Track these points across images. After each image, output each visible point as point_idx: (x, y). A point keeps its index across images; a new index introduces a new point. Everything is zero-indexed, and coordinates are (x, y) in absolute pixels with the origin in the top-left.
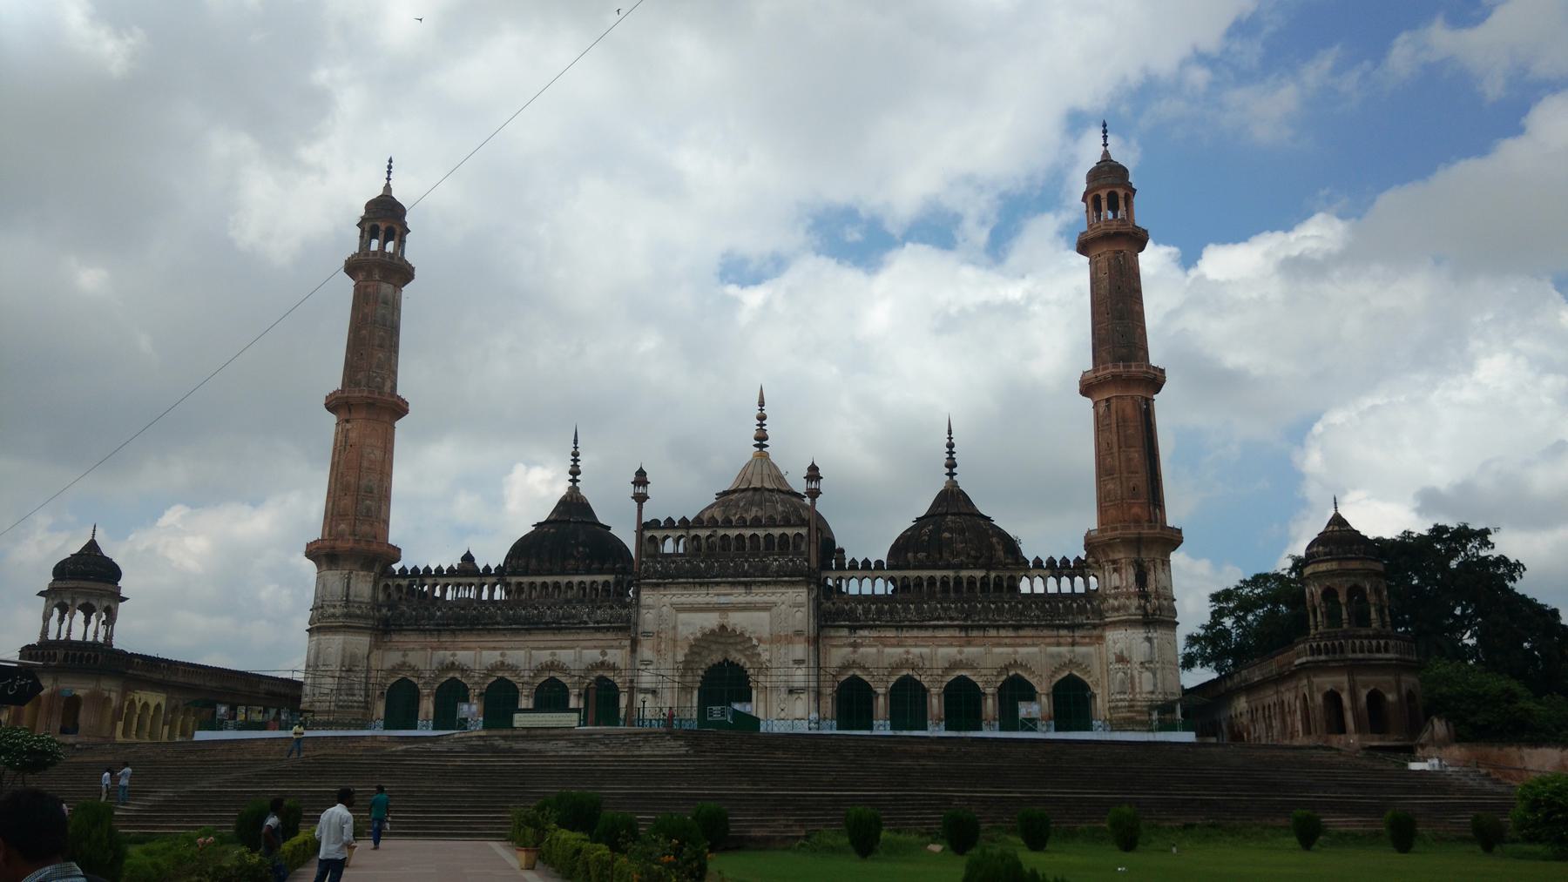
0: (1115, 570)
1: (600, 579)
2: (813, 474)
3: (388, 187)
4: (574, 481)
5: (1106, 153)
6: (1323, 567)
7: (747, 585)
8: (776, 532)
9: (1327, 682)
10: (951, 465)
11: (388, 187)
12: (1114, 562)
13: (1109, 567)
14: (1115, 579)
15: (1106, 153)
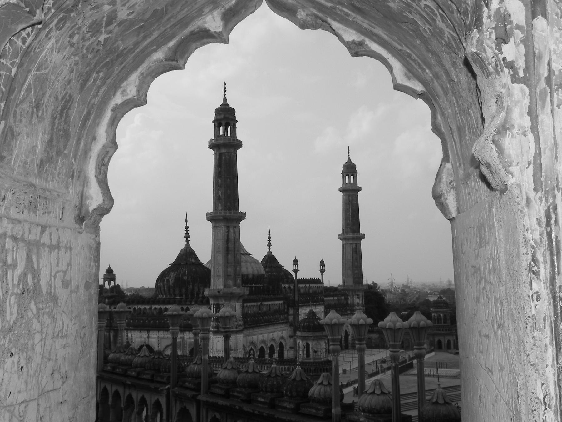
0: (358, 298)
1: (281, 302)
2: (322, 263)
3: (225, 100)
4: (187, 241)
5: (349, 159)
6: (445, 310)
7: (315, 305)
8: (319, 285)
9: (447, 338)
10: (269, 245)
11: (225, 100)
12: (358, 295)
13: (356, 296)
14: (357, 300)
15: (349, 159)
